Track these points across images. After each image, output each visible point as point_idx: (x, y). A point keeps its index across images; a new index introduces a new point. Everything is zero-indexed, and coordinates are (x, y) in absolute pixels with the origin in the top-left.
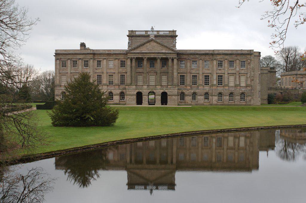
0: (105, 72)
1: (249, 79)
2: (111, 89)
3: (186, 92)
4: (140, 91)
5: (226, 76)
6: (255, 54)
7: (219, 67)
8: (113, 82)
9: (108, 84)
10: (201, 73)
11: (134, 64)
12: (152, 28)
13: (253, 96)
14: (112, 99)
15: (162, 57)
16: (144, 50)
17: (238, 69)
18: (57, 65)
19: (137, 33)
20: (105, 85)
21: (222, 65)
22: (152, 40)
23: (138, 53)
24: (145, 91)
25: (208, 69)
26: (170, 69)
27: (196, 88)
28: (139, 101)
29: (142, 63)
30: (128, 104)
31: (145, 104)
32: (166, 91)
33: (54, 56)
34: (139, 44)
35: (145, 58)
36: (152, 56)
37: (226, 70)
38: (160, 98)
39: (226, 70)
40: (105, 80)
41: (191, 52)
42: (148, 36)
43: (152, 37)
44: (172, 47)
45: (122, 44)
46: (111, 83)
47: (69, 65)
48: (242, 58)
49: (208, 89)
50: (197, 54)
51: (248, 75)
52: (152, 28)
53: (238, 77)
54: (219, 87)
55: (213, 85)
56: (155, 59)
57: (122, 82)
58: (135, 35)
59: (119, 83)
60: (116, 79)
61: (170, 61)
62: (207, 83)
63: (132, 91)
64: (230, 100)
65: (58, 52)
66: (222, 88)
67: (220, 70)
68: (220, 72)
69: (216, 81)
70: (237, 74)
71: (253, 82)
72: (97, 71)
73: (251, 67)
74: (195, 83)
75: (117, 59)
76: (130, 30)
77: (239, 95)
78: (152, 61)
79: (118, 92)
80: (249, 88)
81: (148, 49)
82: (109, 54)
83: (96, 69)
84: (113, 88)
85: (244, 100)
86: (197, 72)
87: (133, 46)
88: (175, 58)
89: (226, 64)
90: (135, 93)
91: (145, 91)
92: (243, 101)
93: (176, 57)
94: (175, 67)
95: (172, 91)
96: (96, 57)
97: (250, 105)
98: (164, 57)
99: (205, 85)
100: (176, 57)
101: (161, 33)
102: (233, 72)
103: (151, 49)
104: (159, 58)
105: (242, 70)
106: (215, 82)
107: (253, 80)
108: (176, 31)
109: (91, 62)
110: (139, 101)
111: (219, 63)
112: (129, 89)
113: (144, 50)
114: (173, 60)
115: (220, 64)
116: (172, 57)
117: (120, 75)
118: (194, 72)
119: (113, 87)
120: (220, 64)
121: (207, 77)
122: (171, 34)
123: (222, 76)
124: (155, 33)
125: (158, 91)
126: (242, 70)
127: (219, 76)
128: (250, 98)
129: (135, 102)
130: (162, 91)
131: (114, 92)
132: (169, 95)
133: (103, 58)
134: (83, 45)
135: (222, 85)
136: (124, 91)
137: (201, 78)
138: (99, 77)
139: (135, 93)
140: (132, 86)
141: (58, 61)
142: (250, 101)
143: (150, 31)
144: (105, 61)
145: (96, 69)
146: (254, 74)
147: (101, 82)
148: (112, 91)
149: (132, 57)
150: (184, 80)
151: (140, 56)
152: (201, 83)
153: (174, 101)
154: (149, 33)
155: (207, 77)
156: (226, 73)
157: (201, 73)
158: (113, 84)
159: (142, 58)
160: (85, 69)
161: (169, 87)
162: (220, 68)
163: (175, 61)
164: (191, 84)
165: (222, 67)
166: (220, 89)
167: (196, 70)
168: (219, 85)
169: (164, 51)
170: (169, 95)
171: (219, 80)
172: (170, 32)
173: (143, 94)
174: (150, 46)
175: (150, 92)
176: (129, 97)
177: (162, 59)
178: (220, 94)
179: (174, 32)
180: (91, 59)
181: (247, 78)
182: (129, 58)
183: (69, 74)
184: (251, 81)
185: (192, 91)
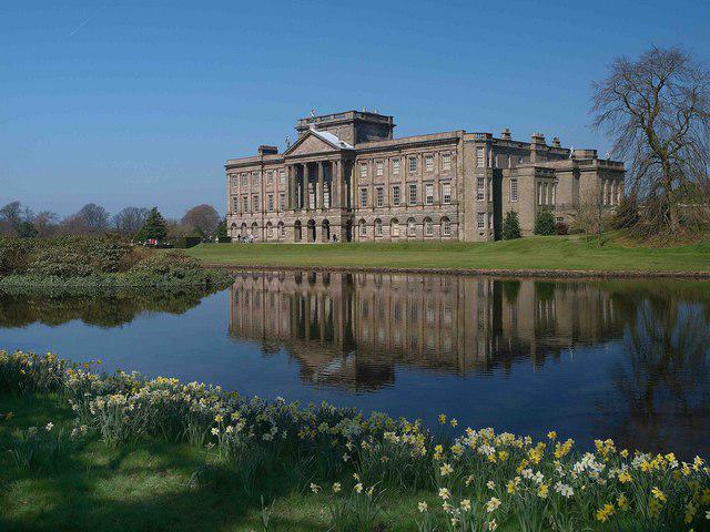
3: (368, 219)
6: (466, 138)
31: (304, 241)
32: (328, 218)
36: (312, 159)
51: (453, 182)
65: (230, 163)
80: (454, 208)
102: (432, 177)
113: (301, 150)
118: (378, 182)
130: (323, 218)
137: (386, 191)
166: (411, 212)
169: (326, 150)
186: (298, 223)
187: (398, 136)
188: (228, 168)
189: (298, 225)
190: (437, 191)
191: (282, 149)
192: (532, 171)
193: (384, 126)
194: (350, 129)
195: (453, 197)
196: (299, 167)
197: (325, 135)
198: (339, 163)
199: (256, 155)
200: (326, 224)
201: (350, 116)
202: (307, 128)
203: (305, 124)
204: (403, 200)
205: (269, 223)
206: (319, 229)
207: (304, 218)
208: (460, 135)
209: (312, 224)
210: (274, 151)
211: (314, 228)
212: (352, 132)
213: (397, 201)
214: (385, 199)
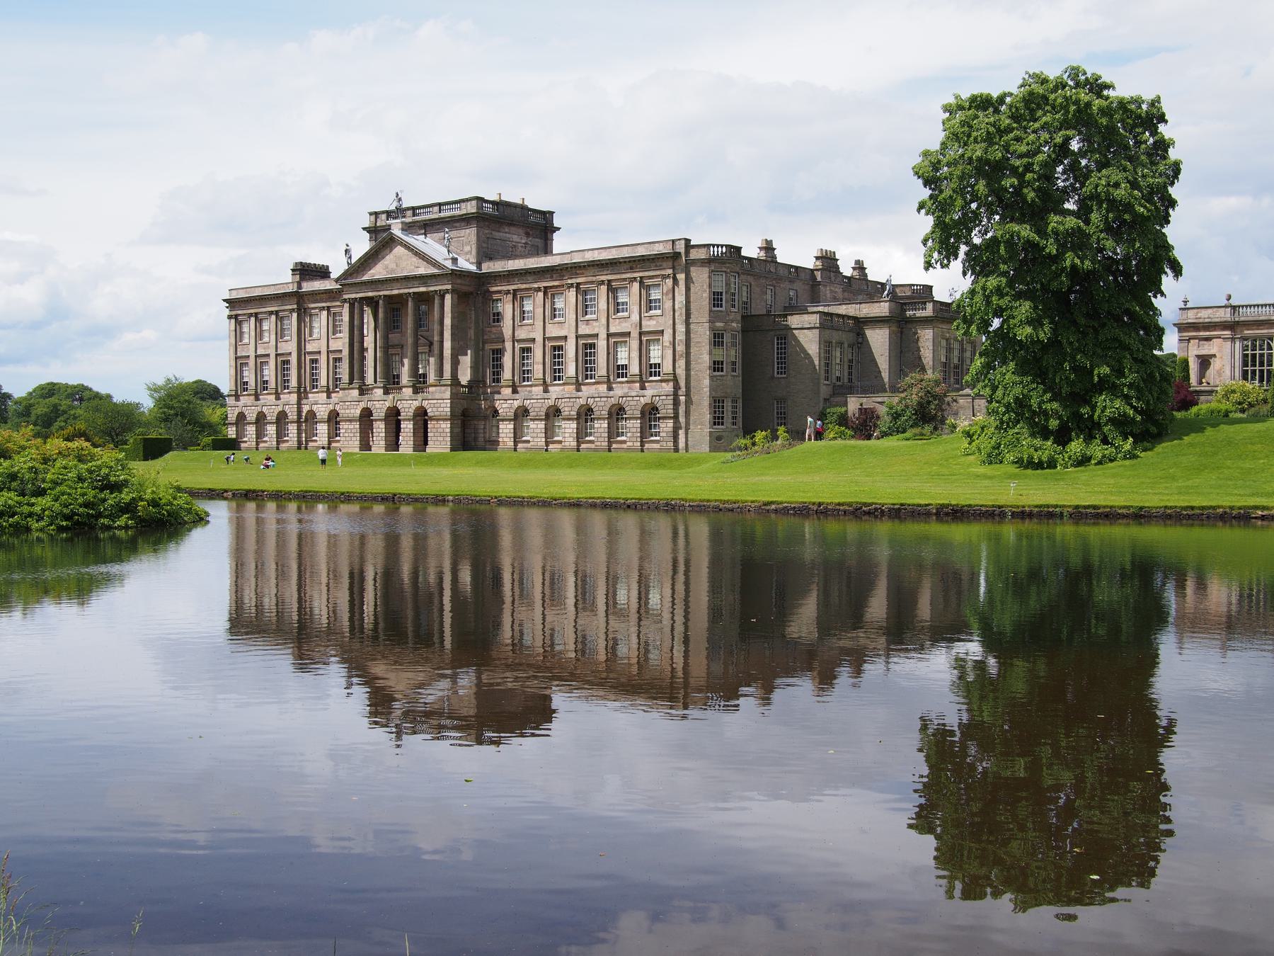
1: (669, 352)
5: (602, 344)
6: (694, 254)
10: (539, 339)
24: (408, 403)
32: (425, 403)
39: (604, 321)
48: (647, 274)
51: (667, 337)
53: (635, 344)
65: (235, 295)
68: (588, 332)
70: (635, 334)
72: (310, 348)
86: (531, 336)
88: (447, 291)
90: (358, 412)
91: (378, 405)
93: (449, 287)
102: (624, 327)
103: (393, 266)
114: (442, 297)
127: (585, 345)
130: (416, 404)
132: (432, 419)
148: (337, 408)
156: (603, 335)
183: (252, 362)
185: (516, 404)
186: (366, 415)
187: (564, 246)
188: (232, 303)
189: (366, 417)
190: (635, 354)
191: (338, 267)
192: (814, 319)
193: (539, 227)
194: (469, 235)
195: (667, 367)
196: (372, 302)
197: (418, 241)
199: (283, 278)
200: (422, 418)
201: (471, 208)
202: (388, 228)
203: (382, 221)
204: (571, 370)
205: (312, 414)
206: (407, 427)
207: (380, 402)
208: (681, 247)
209: (393, 417)
210: (323, 273)
211: (398, 423)
212: (474, 238)
213: (557, 374)
214: (538, 371)
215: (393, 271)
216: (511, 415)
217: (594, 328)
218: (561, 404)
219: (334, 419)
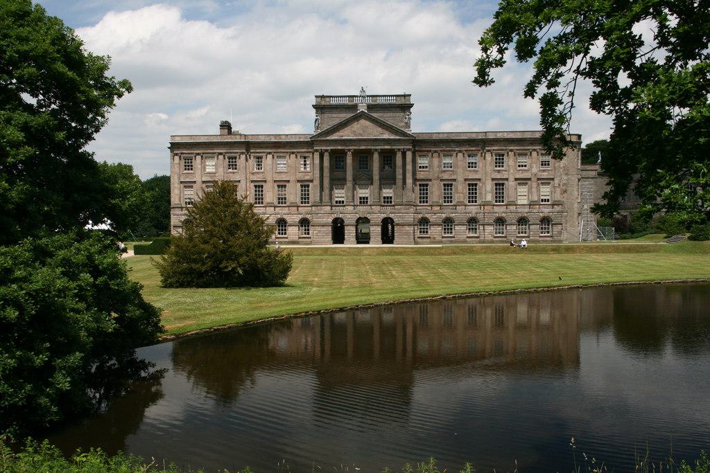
0: (269, 178)
1: (558, 190)
2: (282, 212)
3: (432, 218)
4: (341, 216)
7: (496, 166)
8: (285, 198)
9: (276, 204)
10: (460, 178)
11: (326, 163)
12: (363, 90)
13: (566, 223)
14: (285, 233)
15: (382, 147)
16: (346, 134)
17: (535, 170)
18: (176, 166)
19: (333, 102)
20: (270, 205)
21: (503, 163)
22: (362, 116)
23: (336, 141)
25: (474, 171)
26: (399, 171)
27: (451, 209)
28: (338, 236)
29: (343, 161)
30: (317, 243)
33: (169, 148)
34: (337, 121)
35: (349, 150)
37: (512, 171)
38: (380, 229)
39: (512, 171)
40: (270, 195)
41: (441, 137)
42: (355, 107)
43: (362, 108)
44: (402, 127)
45: (302, 124)
46: (282, 200)
47: (199, 166)
49: (474, 211)
50: (453, 141)
52: (363, 90)
53: (534, 185)
54: (496, 205)
55: (485, 204)
56: (369, 153)
57: (305, 199)
58: (328, 104)
59: (298, 201)
60: (293, 193)
61: (399, 156)
62: (472, 198)
63: (325, 216)
64: (519, 233)
65: (178, 140)
66: (503, 209)
67: (499, 171)
68: (499, 176)
69: (490, 194)
70: (534, 179)
71: (565, 195)
73: (561, 166)
74: (448, 198)
75: (293, 153)
76: (319, 95)
77: (538, 222)
78: (363, 157)
79: (297, 218)
80: (557, 208)
81: (354, 132)
82: (280, 146)
83: (253, 174)
84: (286, 210)
85: (548, 232)
87: (326, 127)
88: (409, 150)
89: (510, 161)
90: (330, 220)
91: (349, 216)
92: (546, 234)
93: (411, 147)
94: (409, 167)
95: (404, 216)
96: (252, 151)
97: (560, 241)
98: (386, 147)
99: (469, 202)
100: (411, 147)
101: (380, 101)
103: (361, 132)
104: (376, 150)
105: (544, 171)
106: (489, 197)
107: (565, 191)
108: (410, 95)
109: (241, 161)
110: (338, 236)
111: (496, 159)
112: (320, 212)
113: (346, 134)
115: (499, 161)
116: (402, 147)
117: (299, 184)
119: (287, 209)
120: (499, 161)
121: (473, 186)
122: (400, 103)
123: (503, 184)
124: (370, 101)
125: (375, 216)
126: (544, 171)
128: (560, 227)
129: (329, 238)
131: (289, 219)
132: (398, 225)
133: (265, 151)
134: (226, 126)
135: (503, 202)
136: (308, 216)
138: (259, 187)
139: (329, 220)
140: (323, 207)
141: (177, 158)
142: (560, 233)
143: (357, 96)
144: (270, 156)
145: (253, 174)
146: (568, 180)
147: (262, 199)
148: (285, 217)
149: (324, 148)
150: (427, 194)
151: (340, 148)
152: (462, 200)
153: (406, 237)
154: (356, 101)
155: (473, 186)
156: (512, 179)
157: (460, 178)
158: (285, 203)
159: (344, 150)
160: (231, 175)
161: (396, 207)
162: (498, 168)
163: (409, 155)
164: (441, 201)
165: (503, 166)
166: (500, 211)
167: (452, 173)
168: (496, 202)
170: (398, 225)
171: (496, 193)
172: (398, 99)
173: (346, 222)
174: (359, 126)
175: (360, 219)
176: (319, 228)
177: (382, 153)
178: (500, 221)
179: (407, 98)
180: (243, 153)
181: (554, 187)
182: (317, 151)
184: (561, 194)
190: (534, 190)
198: (409, 155)
215: (360, 135)
216: (440, 221)
217: (503, 175)
218: (480, 216)
219: (304, 223)
